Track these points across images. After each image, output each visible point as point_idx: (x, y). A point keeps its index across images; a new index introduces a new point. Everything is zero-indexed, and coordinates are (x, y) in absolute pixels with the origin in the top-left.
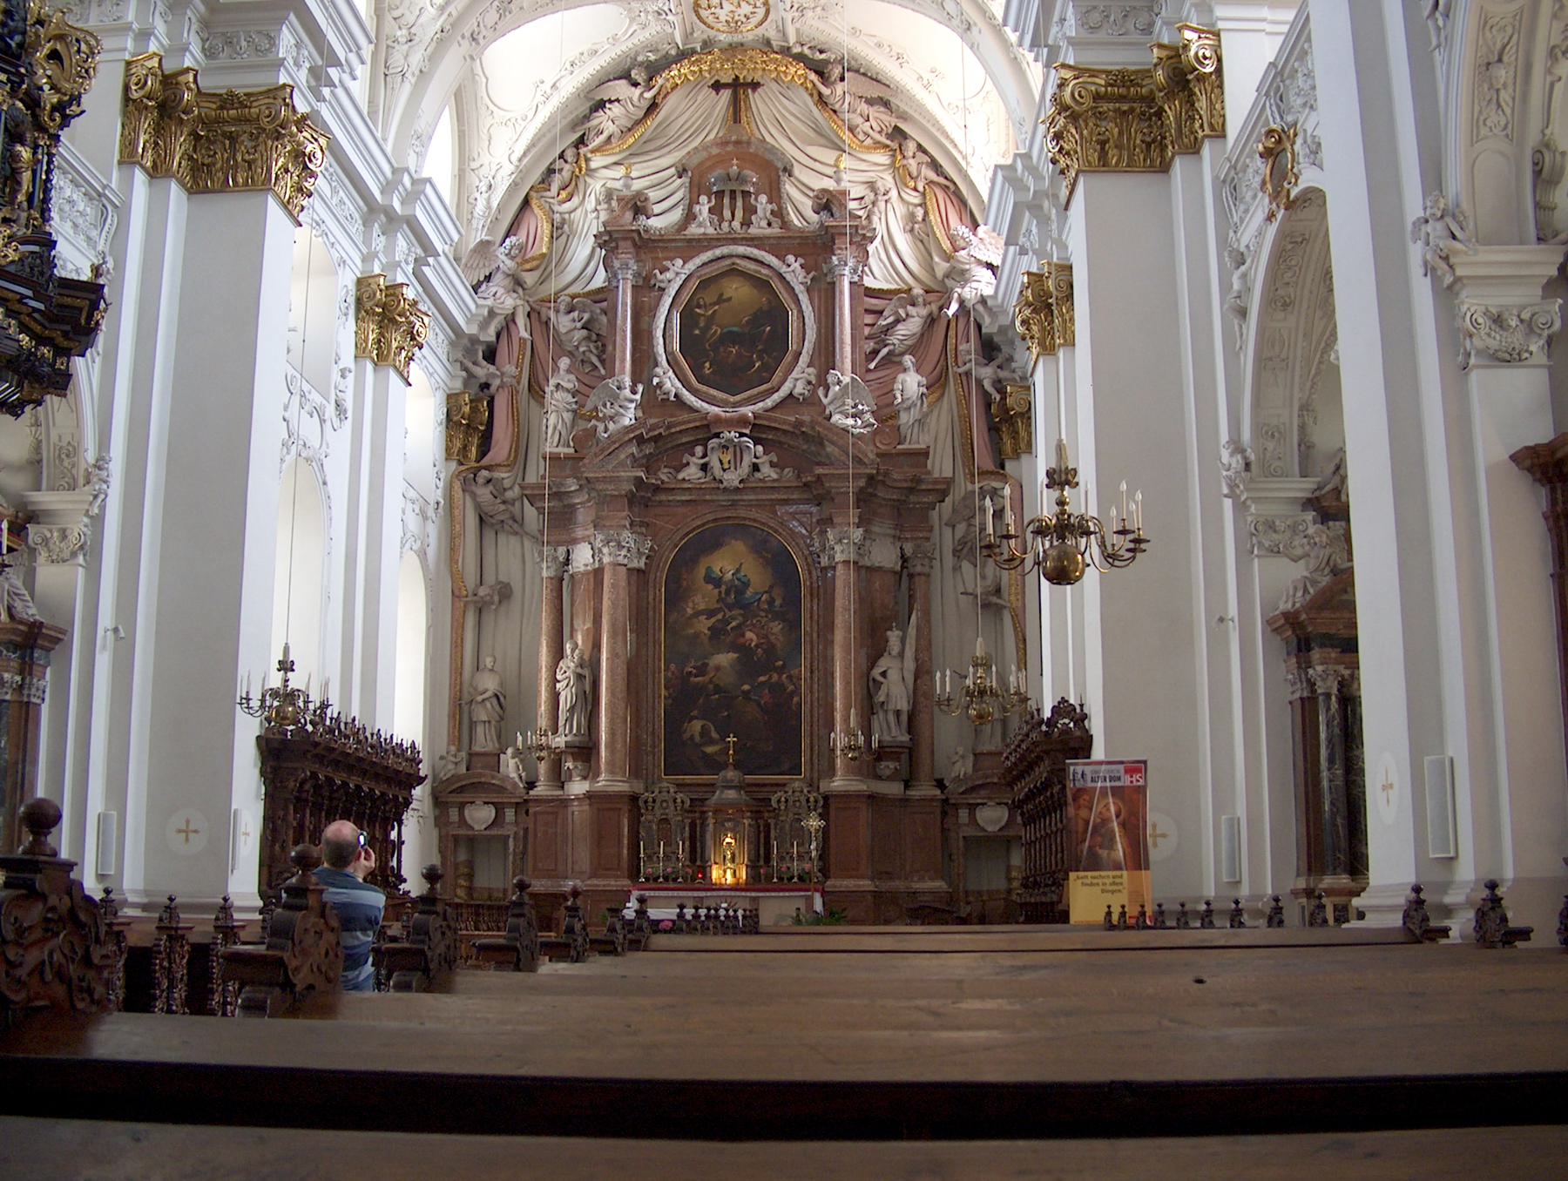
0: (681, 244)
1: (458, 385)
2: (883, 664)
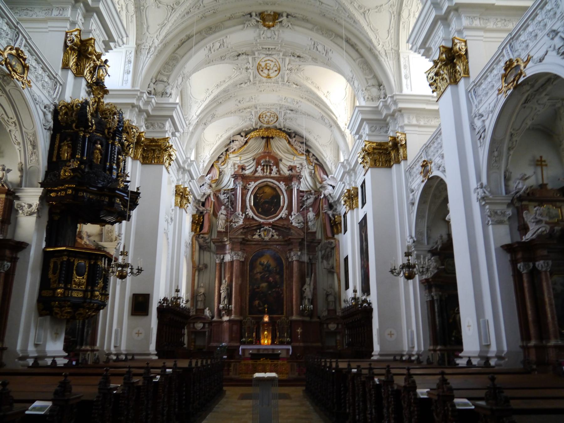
0: (253, 178)
1: (195, 212)
2: (306, 286)
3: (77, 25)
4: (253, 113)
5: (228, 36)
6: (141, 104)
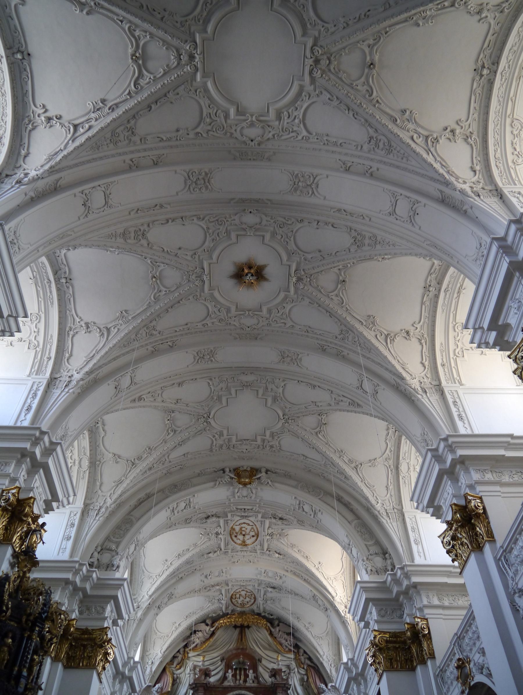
3: (17, 482)
4: (223, 592)
5: (196, 495)
6: (78, 580)
